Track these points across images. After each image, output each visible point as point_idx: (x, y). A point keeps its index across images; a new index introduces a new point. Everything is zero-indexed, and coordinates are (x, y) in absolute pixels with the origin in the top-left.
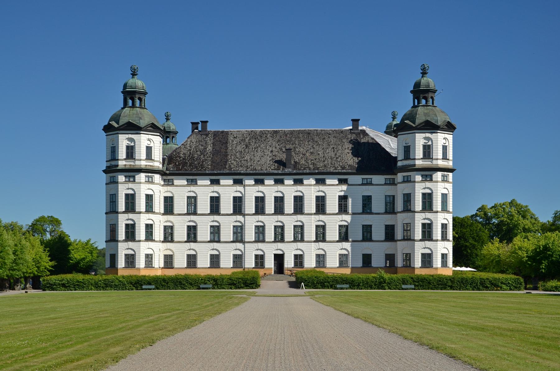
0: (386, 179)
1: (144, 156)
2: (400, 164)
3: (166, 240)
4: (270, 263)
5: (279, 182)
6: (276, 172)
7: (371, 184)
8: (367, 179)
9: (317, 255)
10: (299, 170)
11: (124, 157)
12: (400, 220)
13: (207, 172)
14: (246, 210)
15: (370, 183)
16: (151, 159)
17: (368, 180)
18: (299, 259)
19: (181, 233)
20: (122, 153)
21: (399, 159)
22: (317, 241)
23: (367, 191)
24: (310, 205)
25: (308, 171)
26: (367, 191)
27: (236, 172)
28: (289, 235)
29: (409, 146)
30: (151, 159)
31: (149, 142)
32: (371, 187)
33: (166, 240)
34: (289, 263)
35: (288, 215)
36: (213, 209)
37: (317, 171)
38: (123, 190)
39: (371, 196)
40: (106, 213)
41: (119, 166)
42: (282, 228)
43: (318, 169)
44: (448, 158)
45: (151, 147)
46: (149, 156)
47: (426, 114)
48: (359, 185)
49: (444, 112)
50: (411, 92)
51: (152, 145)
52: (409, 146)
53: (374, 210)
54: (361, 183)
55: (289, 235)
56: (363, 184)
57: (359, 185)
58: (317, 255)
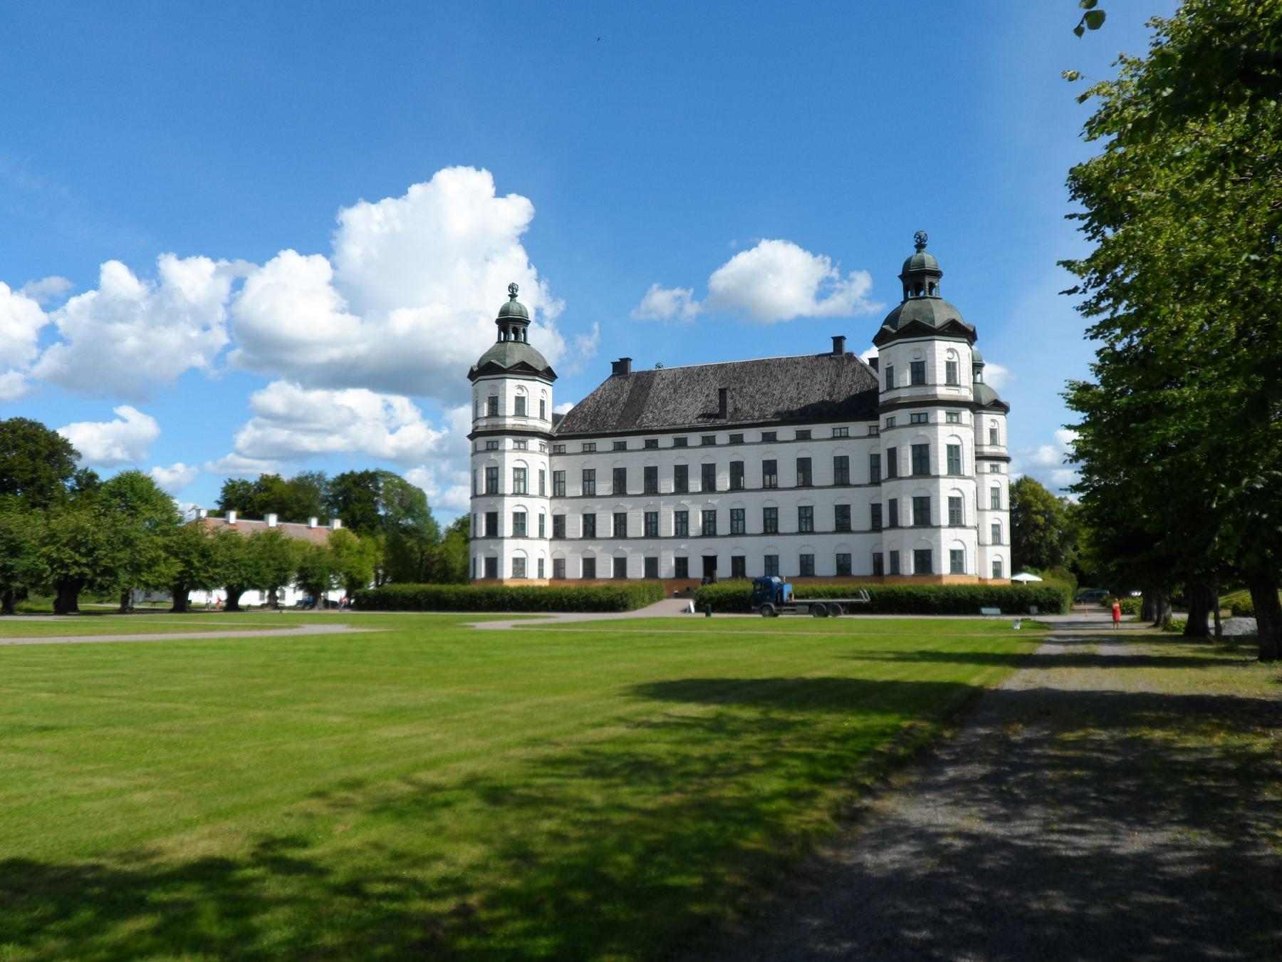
0: (870, 427)
2: (882, 398)
5: (709, 442)
6: (702, 425)
7: (847, 437)
8: (840, 429)
9: (766, 557)
10: (737, 420)
13: (607, 431)
14: (662, 487)
15: (846, 434)
16: (524, 416)
17: (843, 430)
18: (738, 564)
21: (880, 391)
22: (766, 533)
23: (842, 448)
24: (753, 476)
25: (748, 422)
26: (842, 448)
27: (646, 429)
28: (723, 526)
29: (892, 367)
30: (524, 416)
31: (520, 391)
32: (846, 442)
34: (724, 569)
35: (721, 492)
37: (761, 421)
39: (847, 457)
40: (471, 498)
43: (764, 417)
44: (958, 383)
45: (523, 398)
47: (916, 312)
48: (828, 439)
49: (951, 306)
51: (524, 394)
52: (892, 367)
53: (852, 481)
54: (830, 436)
55: (723, 526)
56: (834, 438)
57: (828, 439)
58: (766, 557)
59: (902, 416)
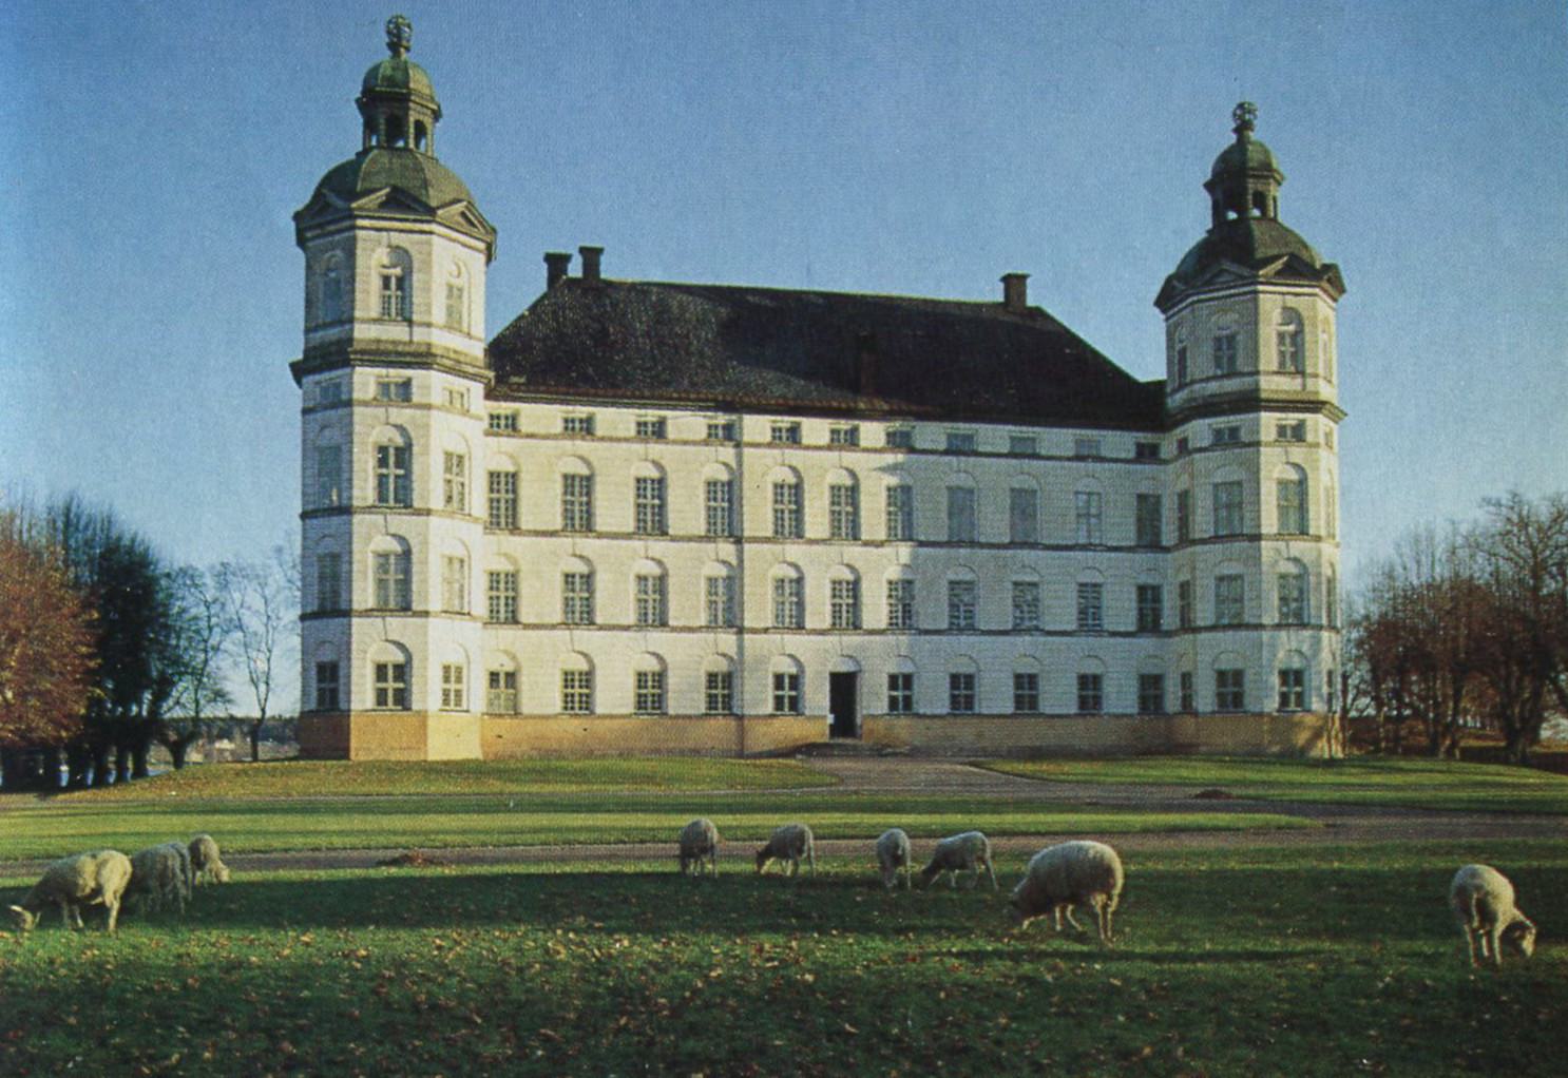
1: (438, 315)
3: (494, 619)
4: (818, 698)
11: (375, 313)
12: (1169, 571)
19: (542, 598)
20: (368, 298)
33: (494, 619)
34: (873, 701)
36: (645, 521)
38: (370, 430)
41: (355, 343)
42: (855, 587)
46: (454, 323)
48: (1069, 459)
50: (1209, 186)
59: (1199, 430)
